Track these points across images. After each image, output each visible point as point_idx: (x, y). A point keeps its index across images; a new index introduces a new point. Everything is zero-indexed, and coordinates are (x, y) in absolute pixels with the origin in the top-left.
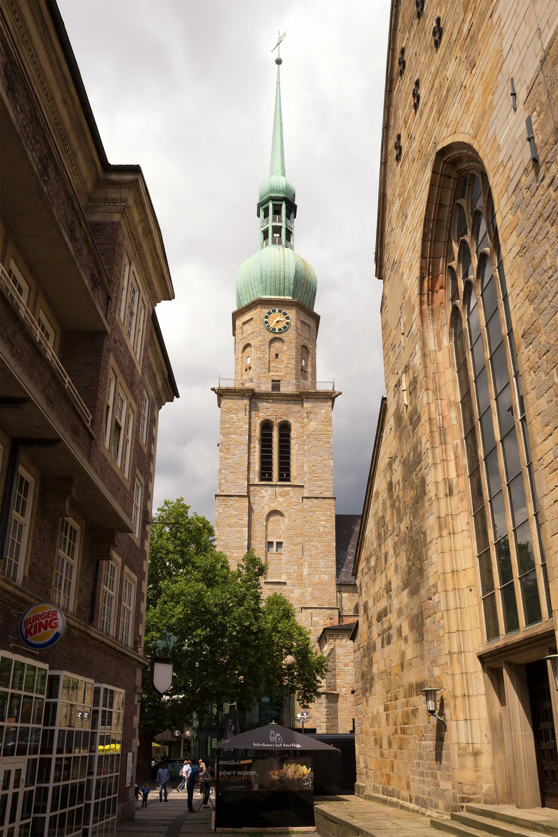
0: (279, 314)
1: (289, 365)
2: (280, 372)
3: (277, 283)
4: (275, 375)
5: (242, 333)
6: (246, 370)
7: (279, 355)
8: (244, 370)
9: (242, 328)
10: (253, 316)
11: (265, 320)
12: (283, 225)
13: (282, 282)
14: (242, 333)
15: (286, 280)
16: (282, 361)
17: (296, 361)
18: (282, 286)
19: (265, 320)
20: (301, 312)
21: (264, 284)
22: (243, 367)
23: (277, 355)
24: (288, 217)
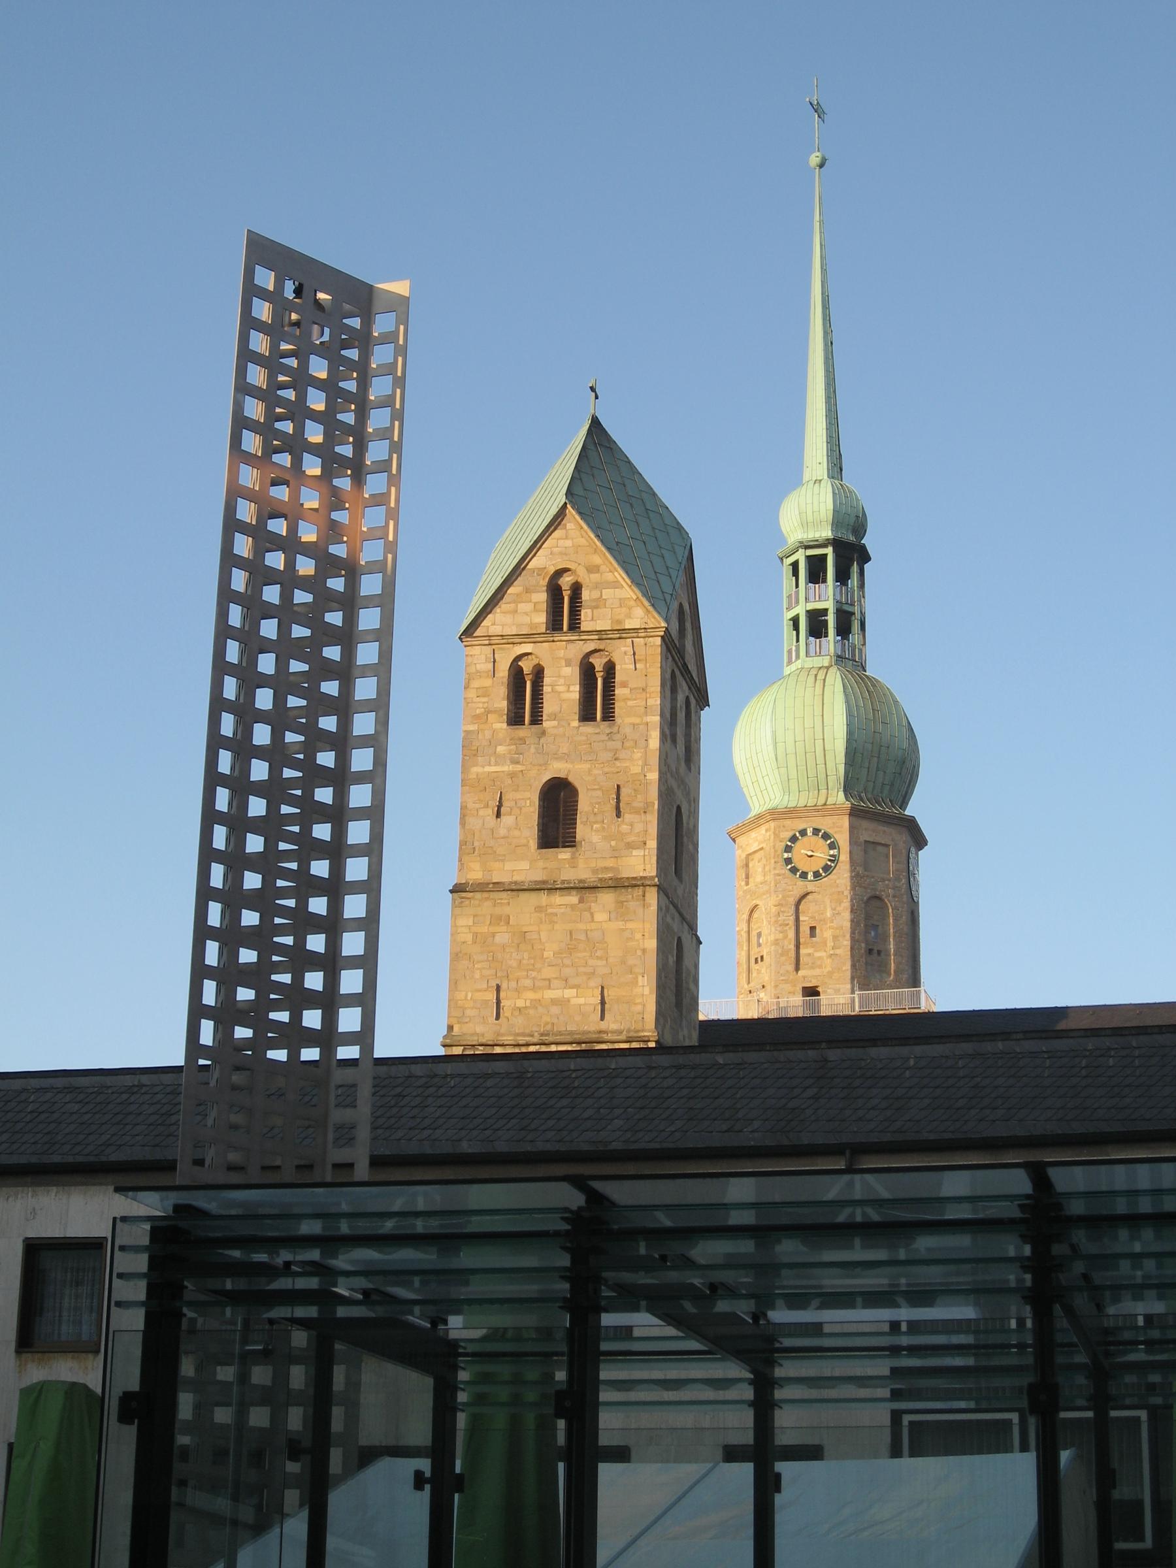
0: (815, 837)
1: (838, 951)
2: (820, 967)
3: (811, 764)
4: (808, 976)
5: (747, 877)
6: (756, 961)
7: (818, 931)
8: (752, 961)
9: (747, 865)
10: (764, 845)
11: (786, 855)
12: (829, 605)
13: (820, 760)
14: (747, 877)
15: (829, 757)
16: (825, 943)
17: (852, 939)
18: (821, 767)
19: (786, 855)
20: (865, 824)
21: (783, 770)
22: (752, 953)
23: (813, 929)
24: (842, 577)
